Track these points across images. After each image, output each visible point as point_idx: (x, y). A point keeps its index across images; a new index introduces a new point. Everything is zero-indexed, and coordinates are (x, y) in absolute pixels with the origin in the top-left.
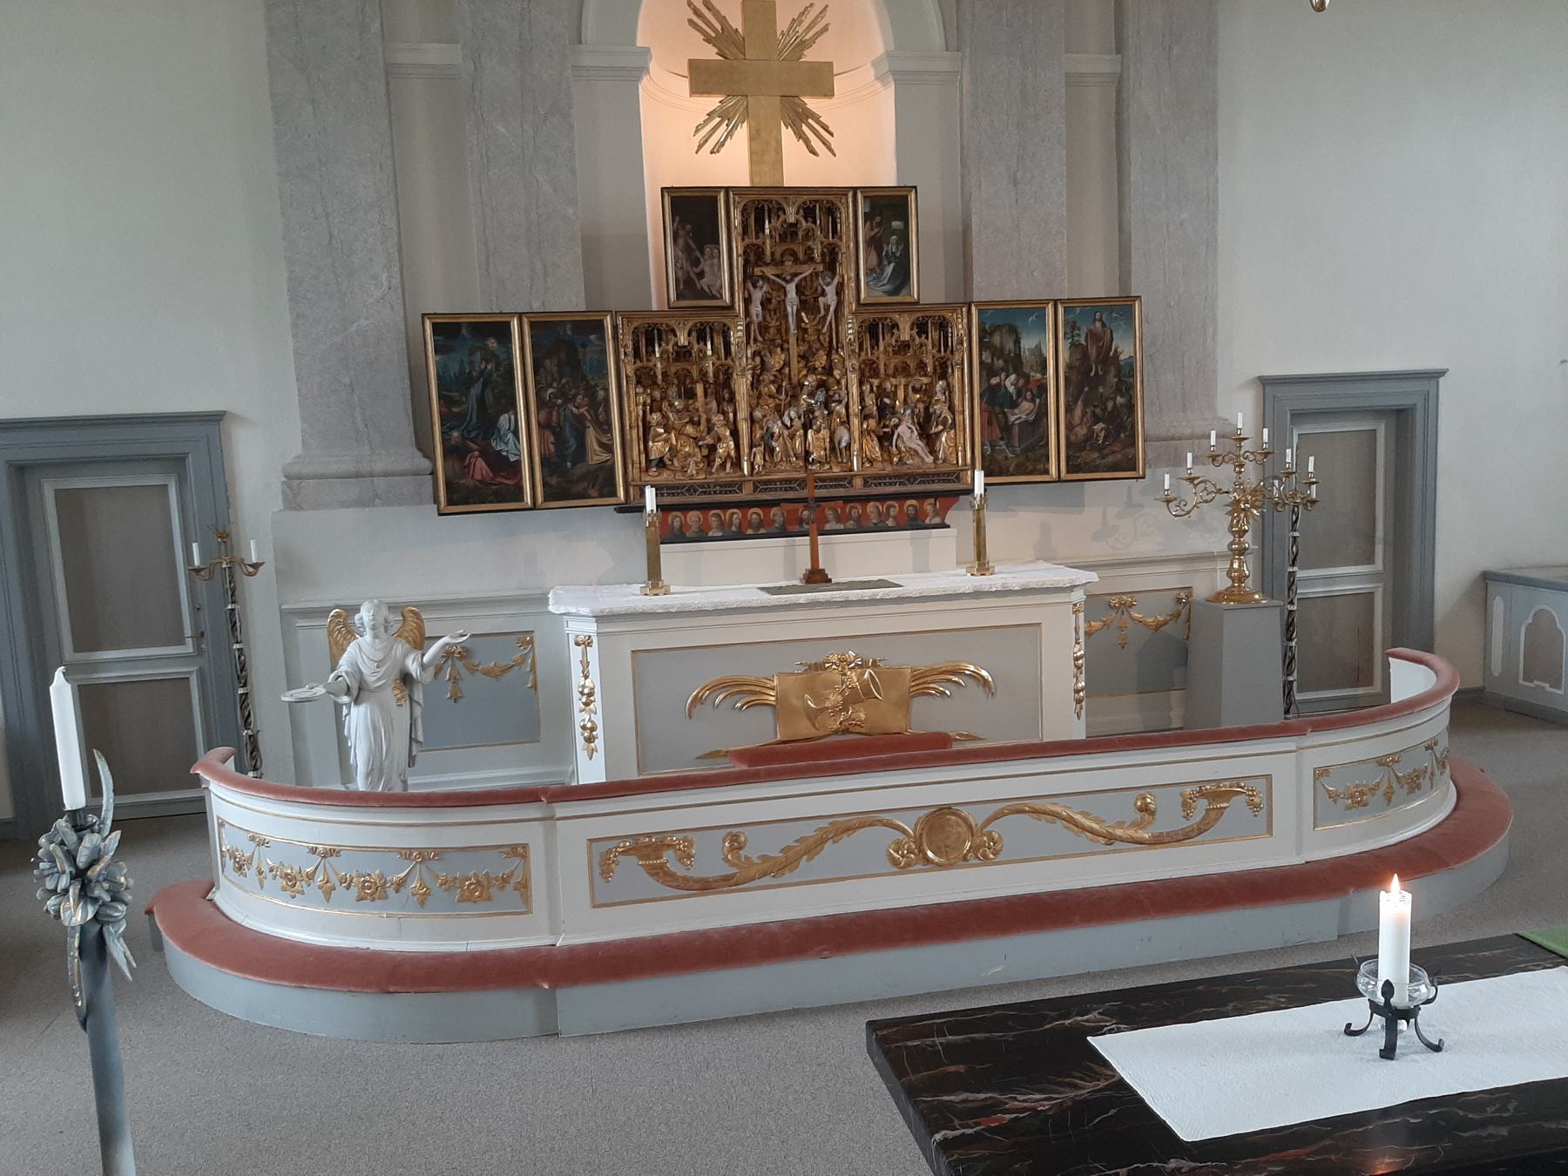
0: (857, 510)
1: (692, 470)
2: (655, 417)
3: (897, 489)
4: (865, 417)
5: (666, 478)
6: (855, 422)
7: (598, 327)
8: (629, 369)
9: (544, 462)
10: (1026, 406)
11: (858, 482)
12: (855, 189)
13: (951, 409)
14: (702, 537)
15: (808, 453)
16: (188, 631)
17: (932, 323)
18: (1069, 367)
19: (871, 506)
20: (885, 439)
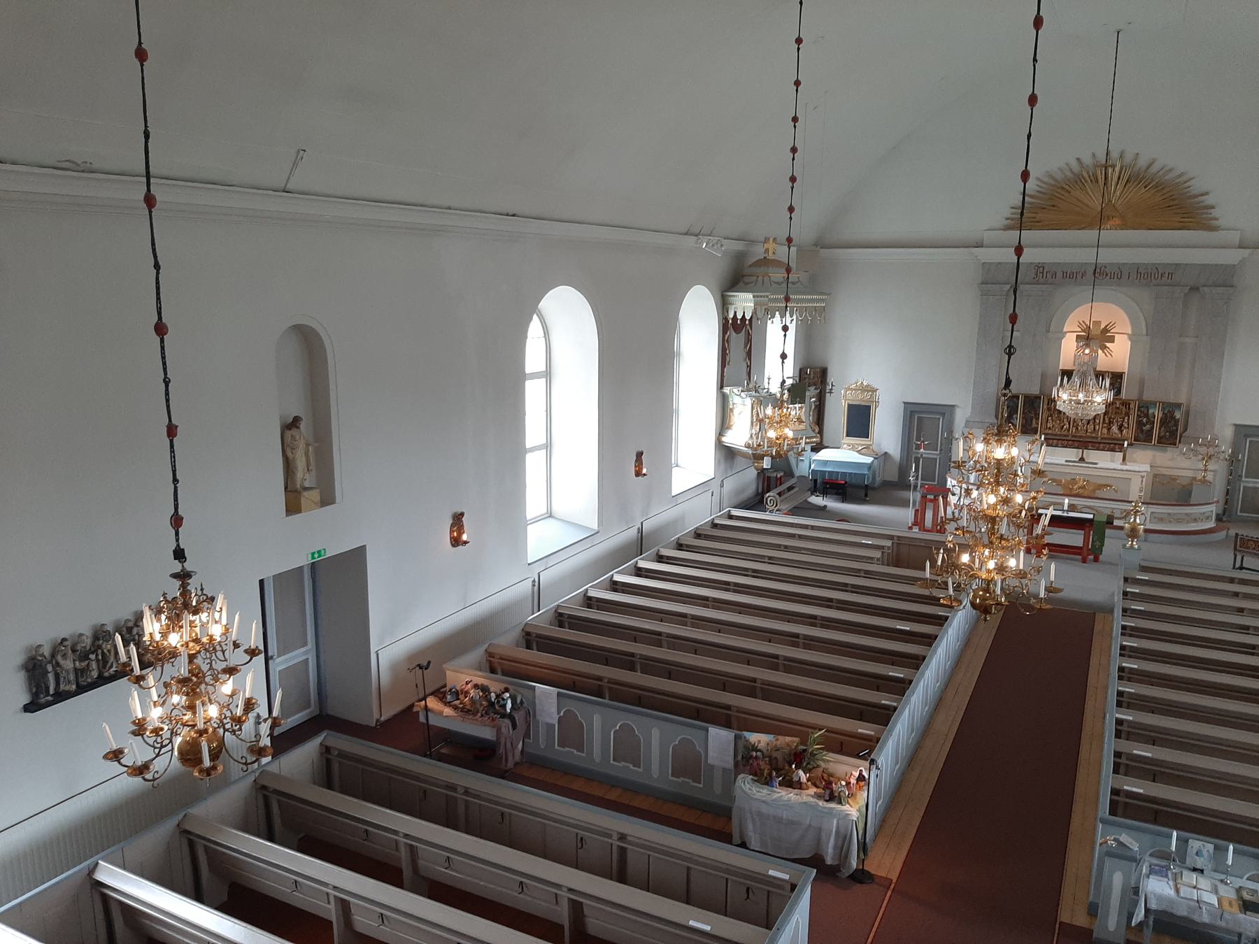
0: (1097, 445)
1: (1057, 430)
2: (1050, 418)
3: (1107, 441)
4: (1104, 422)
5: (1047, 431)
6: (1101, 425)
7: (1040, 397)
8: (1045, 407)
9: (1022, 425)
10: (1148, 426)
11: (1099, 438)
12: (1109, 372)
13: (1128, 424)
14: (1056, 446)
15: (1087, 431)
16: (939, 448)
17: (1126, 404)
18: (1161, 419)
19: (1101, 445)
20: (1109, 429)
